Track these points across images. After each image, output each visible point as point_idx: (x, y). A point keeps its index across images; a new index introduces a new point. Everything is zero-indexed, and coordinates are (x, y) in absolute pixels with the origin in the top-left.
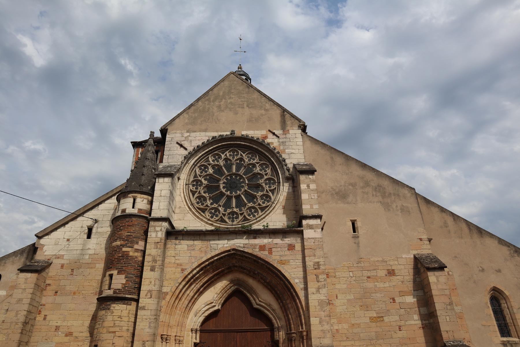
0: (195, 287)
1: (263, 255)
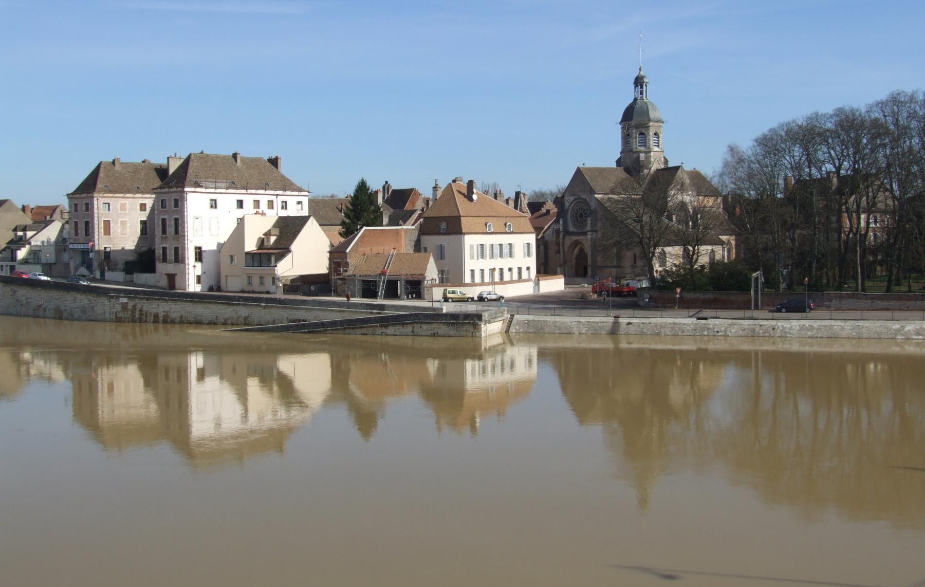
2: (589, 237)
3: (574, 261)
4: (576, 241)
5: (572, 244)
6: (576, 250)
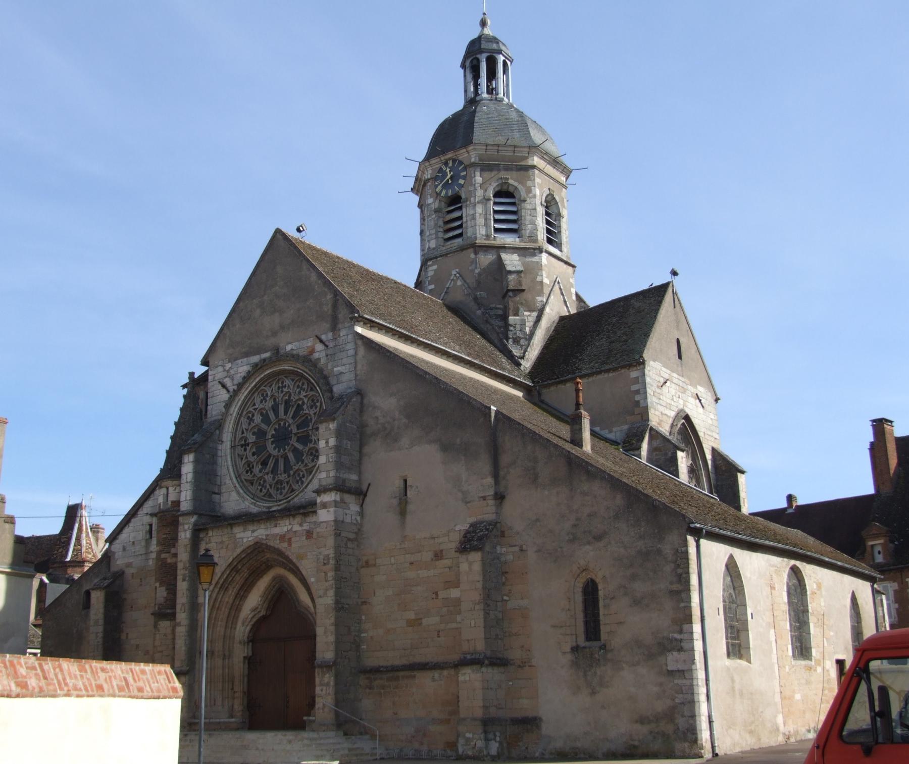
0: (232, 592)
1: (283, 546)
2: (325, 516)
3: (240, 652)
4: (258, 547)
6: (254, 599)
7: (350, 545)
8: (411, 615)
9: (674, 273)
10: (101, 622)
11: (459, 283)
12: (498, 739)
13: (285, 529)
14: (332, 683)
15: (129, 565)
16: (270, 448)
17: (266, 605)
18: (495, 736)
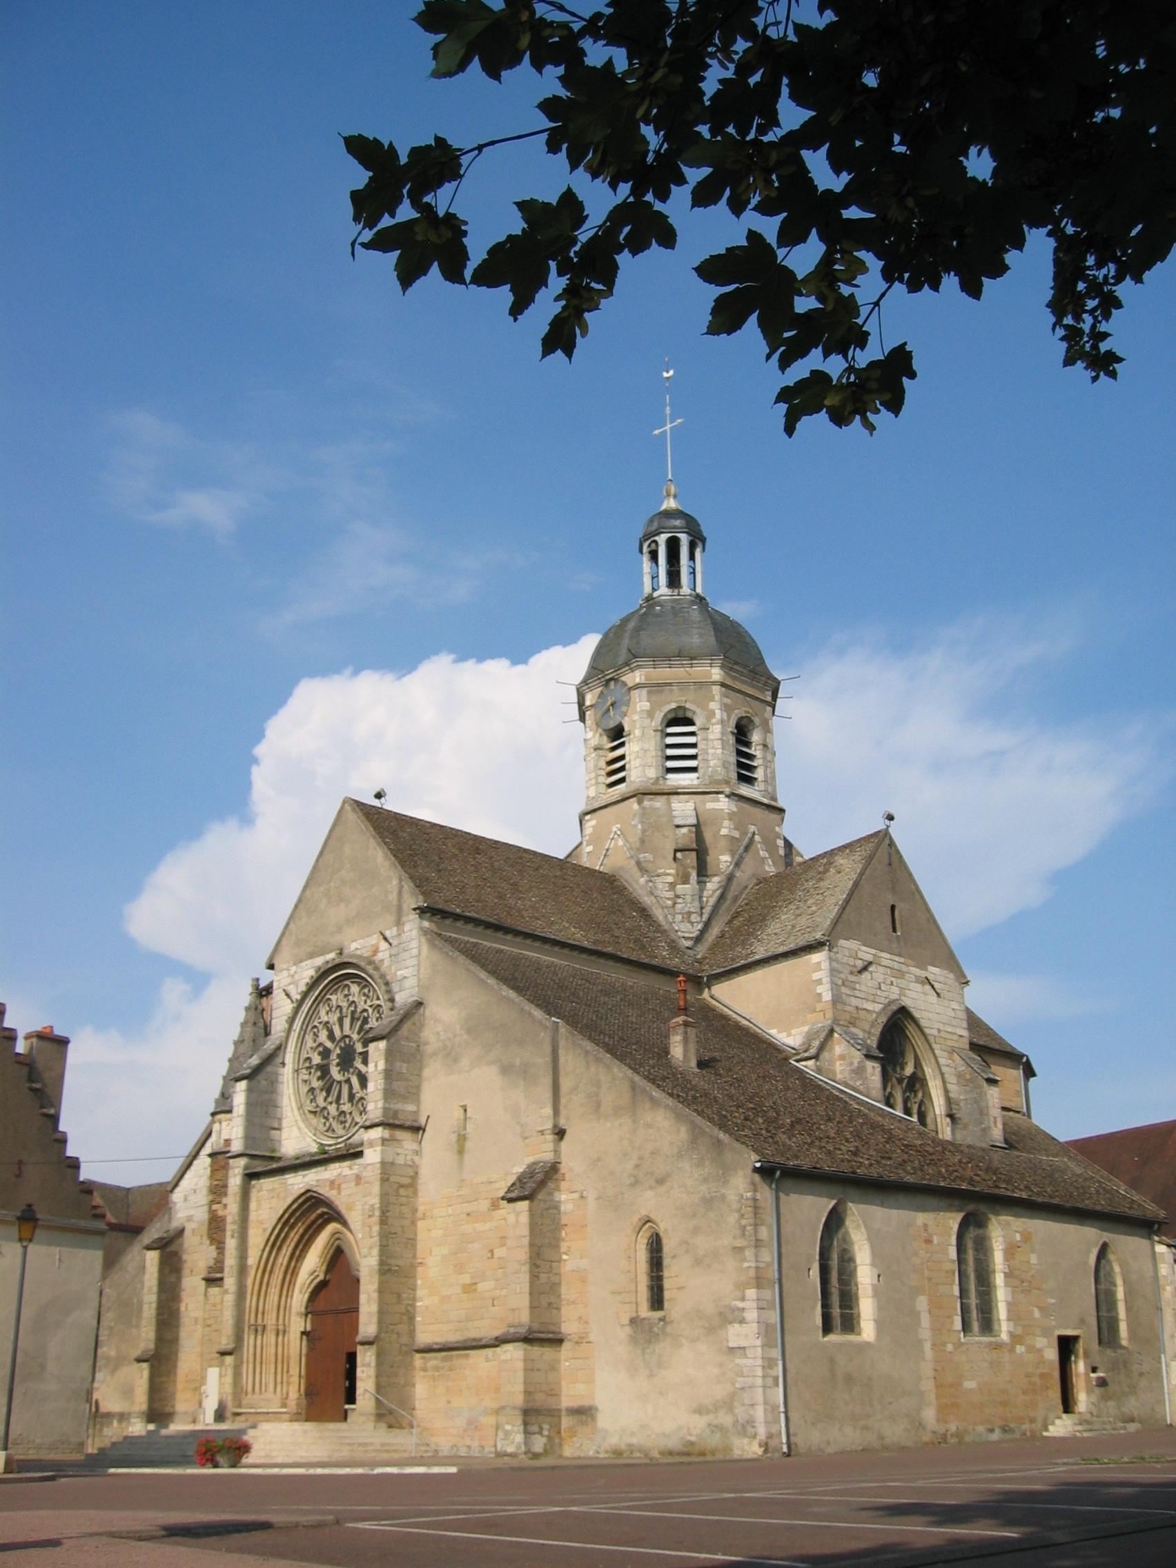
0: (287, 1251)
2: (372, 1156)
5: (288, 1221)
6: (313, 1262)
7: (402, 1191)
8: (466, 1279)
9: (890, 818)
10: (155, 1289)
11: (621, 843)
12: (546, 1433)
13: (335, 1173)
14: (373, 1364)
15: (190, 1219)
16: (335, 1072)
17: (324, 1268)
18: (541, 1429)
